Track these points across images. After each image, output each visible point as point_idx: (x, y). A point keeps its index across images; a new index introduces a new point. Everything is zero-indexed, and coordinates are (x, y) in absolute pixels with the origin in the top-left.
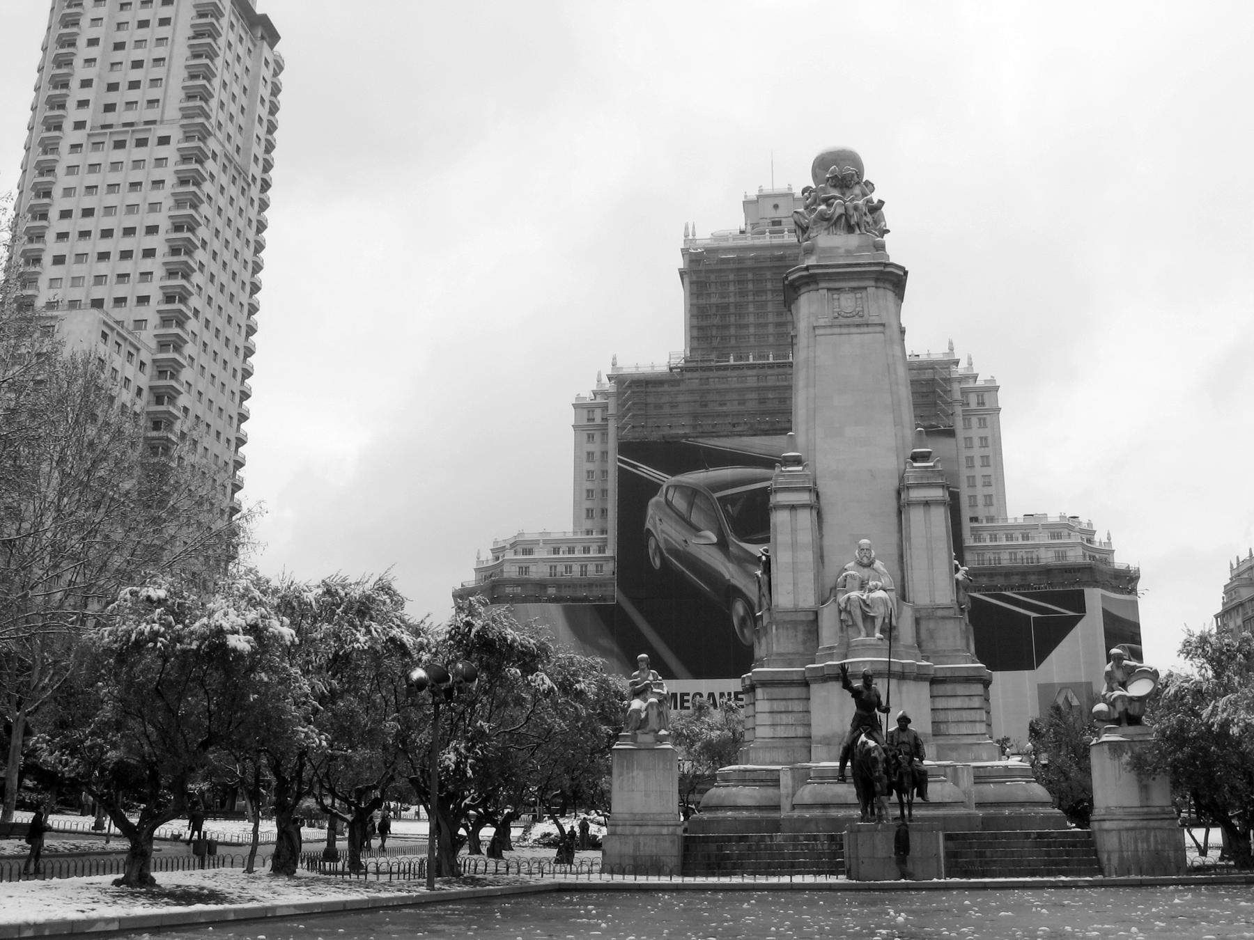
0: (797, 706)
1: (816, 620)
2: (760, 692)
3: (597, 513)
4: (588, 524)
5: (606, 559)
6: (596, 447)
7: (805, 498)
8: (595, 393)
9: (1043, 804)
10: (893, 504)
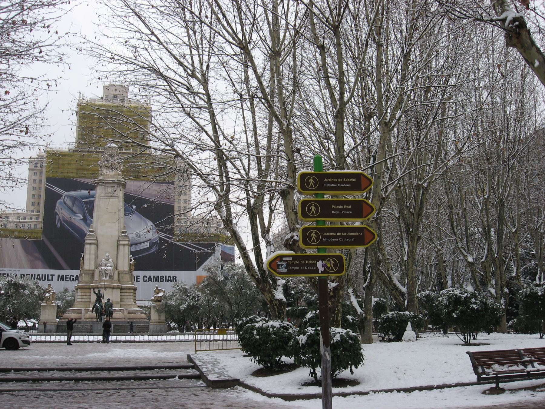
0: (88, 294)
1: (94, 273)
2: (79, 290)
3: (36, 204)
4: (32, 208)
5: (39, 222)
6: (37, 178)
7: (93, 242)
8: (38, 156)
9: (144, 319)
10: (116, 244)
